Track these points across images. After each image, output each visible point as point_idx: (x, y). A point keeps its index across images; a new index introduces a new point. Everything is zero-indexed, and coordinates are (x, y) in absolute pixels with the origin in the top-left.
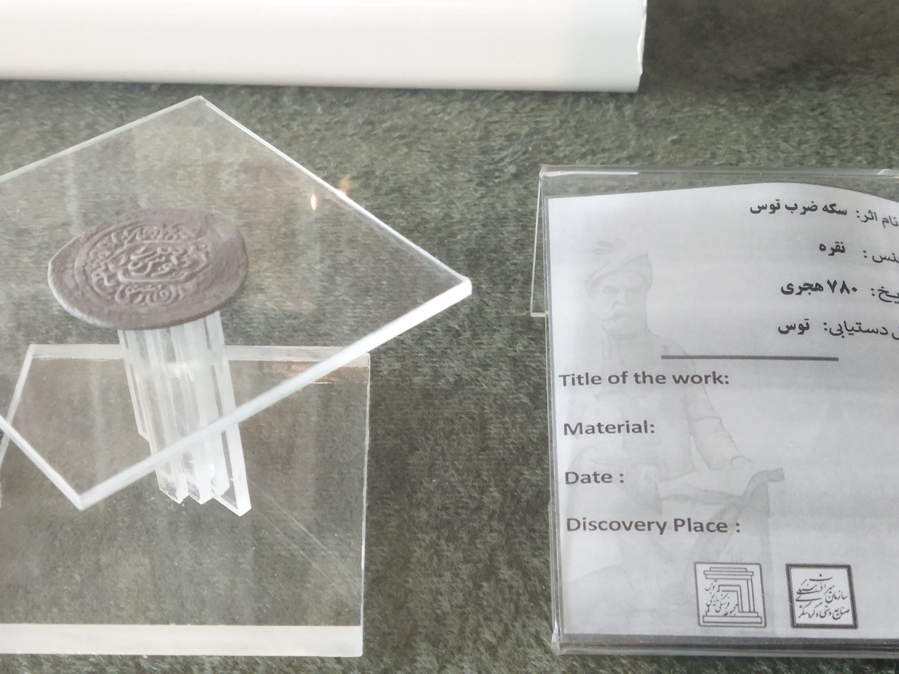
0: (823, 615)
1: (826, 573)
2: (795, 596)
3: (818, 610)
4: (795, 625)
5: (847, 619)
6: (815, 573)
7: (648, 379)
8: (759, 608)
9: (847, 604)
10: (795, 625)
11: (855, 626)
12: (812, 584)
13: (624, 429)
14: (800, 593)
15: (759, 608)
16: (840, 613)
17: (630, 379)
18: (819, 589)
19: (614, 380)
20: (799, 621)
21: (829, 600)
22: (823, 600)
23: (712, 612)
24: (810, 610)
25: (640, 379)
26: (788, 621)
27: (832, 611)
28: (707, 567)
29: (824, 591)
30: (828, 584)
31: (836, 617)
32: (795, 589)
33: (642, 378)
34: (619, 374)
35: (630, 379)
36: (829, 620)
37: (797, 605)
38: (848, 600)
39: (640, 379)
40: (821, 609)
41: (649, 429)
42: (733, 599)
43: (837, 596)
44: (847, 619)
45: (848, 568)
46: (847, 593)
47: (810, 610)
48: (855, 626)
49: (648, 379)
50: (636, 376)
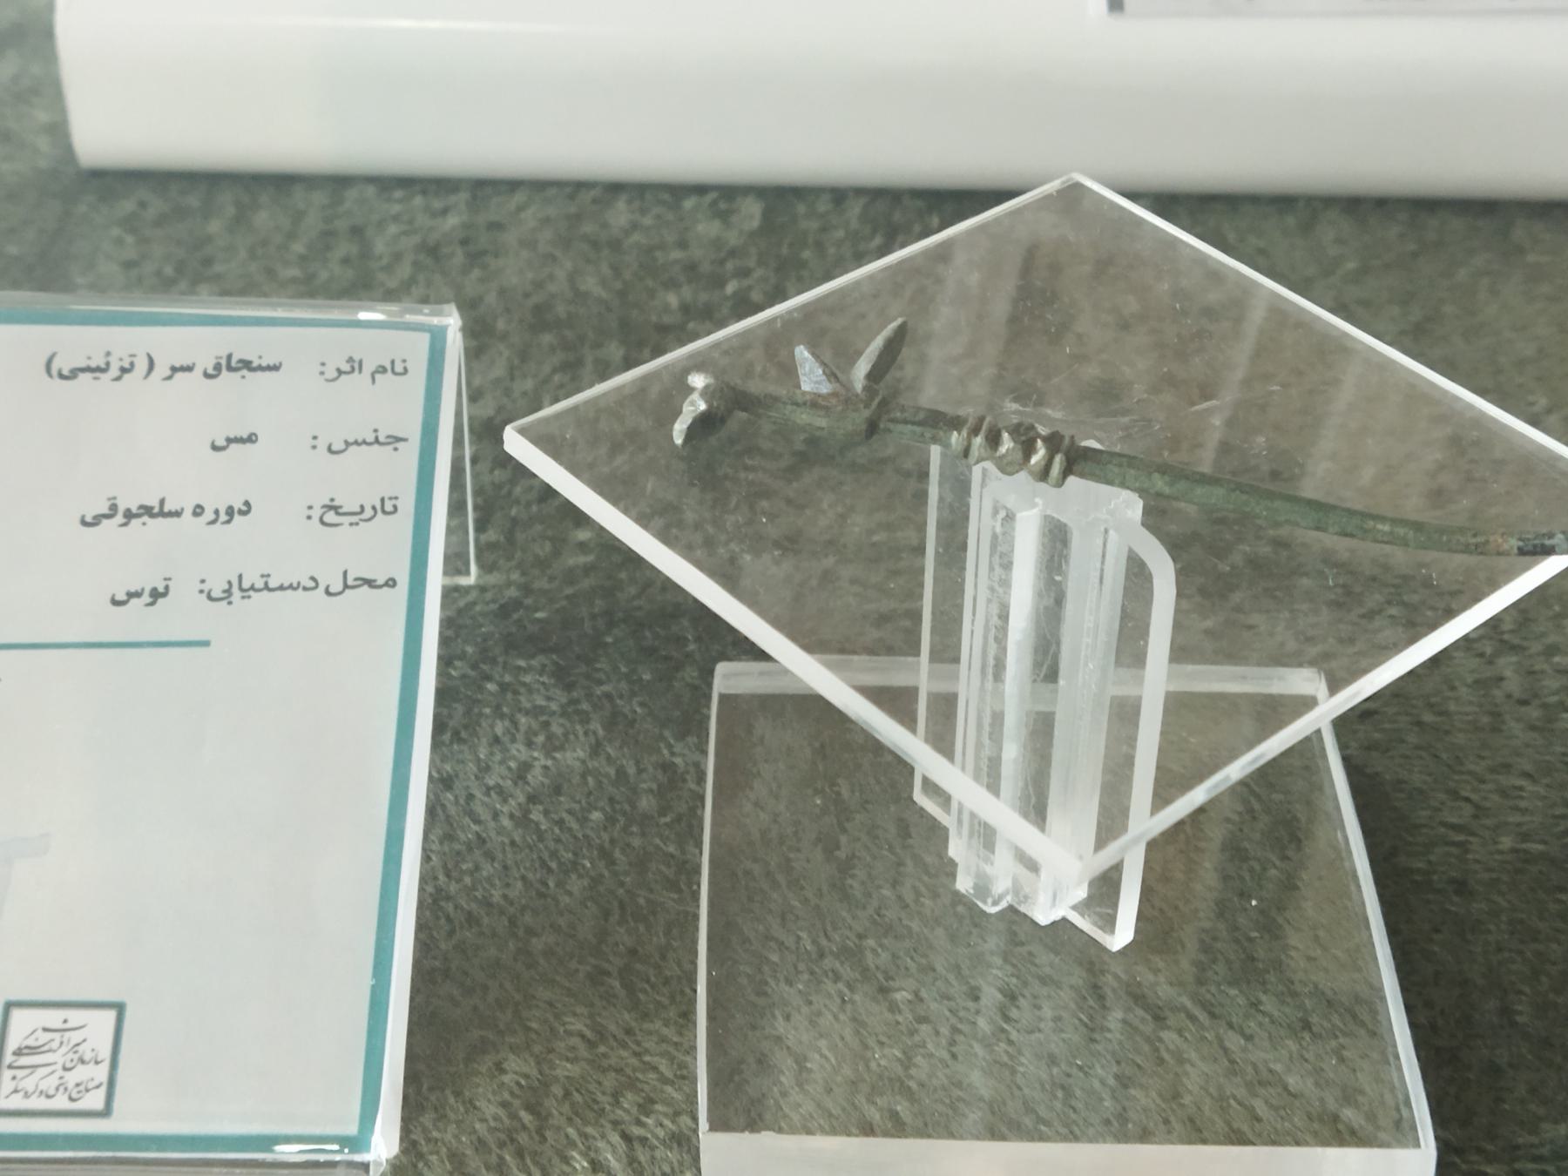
0: (51, 1092)
1: (76, 1017)
3: (43, 1086)
5: (95, 1101)
9: (101, 1073)
11: (106, 1112)
16: (84, 1088)
18: (55, 1045)
21: (69, 1065)
22: (59, 1066)
24: (29, 1084)
27: (71, 1085)
29: (64, 1049)
30: (75, 1037)
31: (74, 1095)
36: (60, 1102)
40: (50, 1084)
43: (87, 1058)
44: (95, 1101)
45: (120, 1008)
46: (105, 1052)
47: (29, 1084)
48: (106, 1112)
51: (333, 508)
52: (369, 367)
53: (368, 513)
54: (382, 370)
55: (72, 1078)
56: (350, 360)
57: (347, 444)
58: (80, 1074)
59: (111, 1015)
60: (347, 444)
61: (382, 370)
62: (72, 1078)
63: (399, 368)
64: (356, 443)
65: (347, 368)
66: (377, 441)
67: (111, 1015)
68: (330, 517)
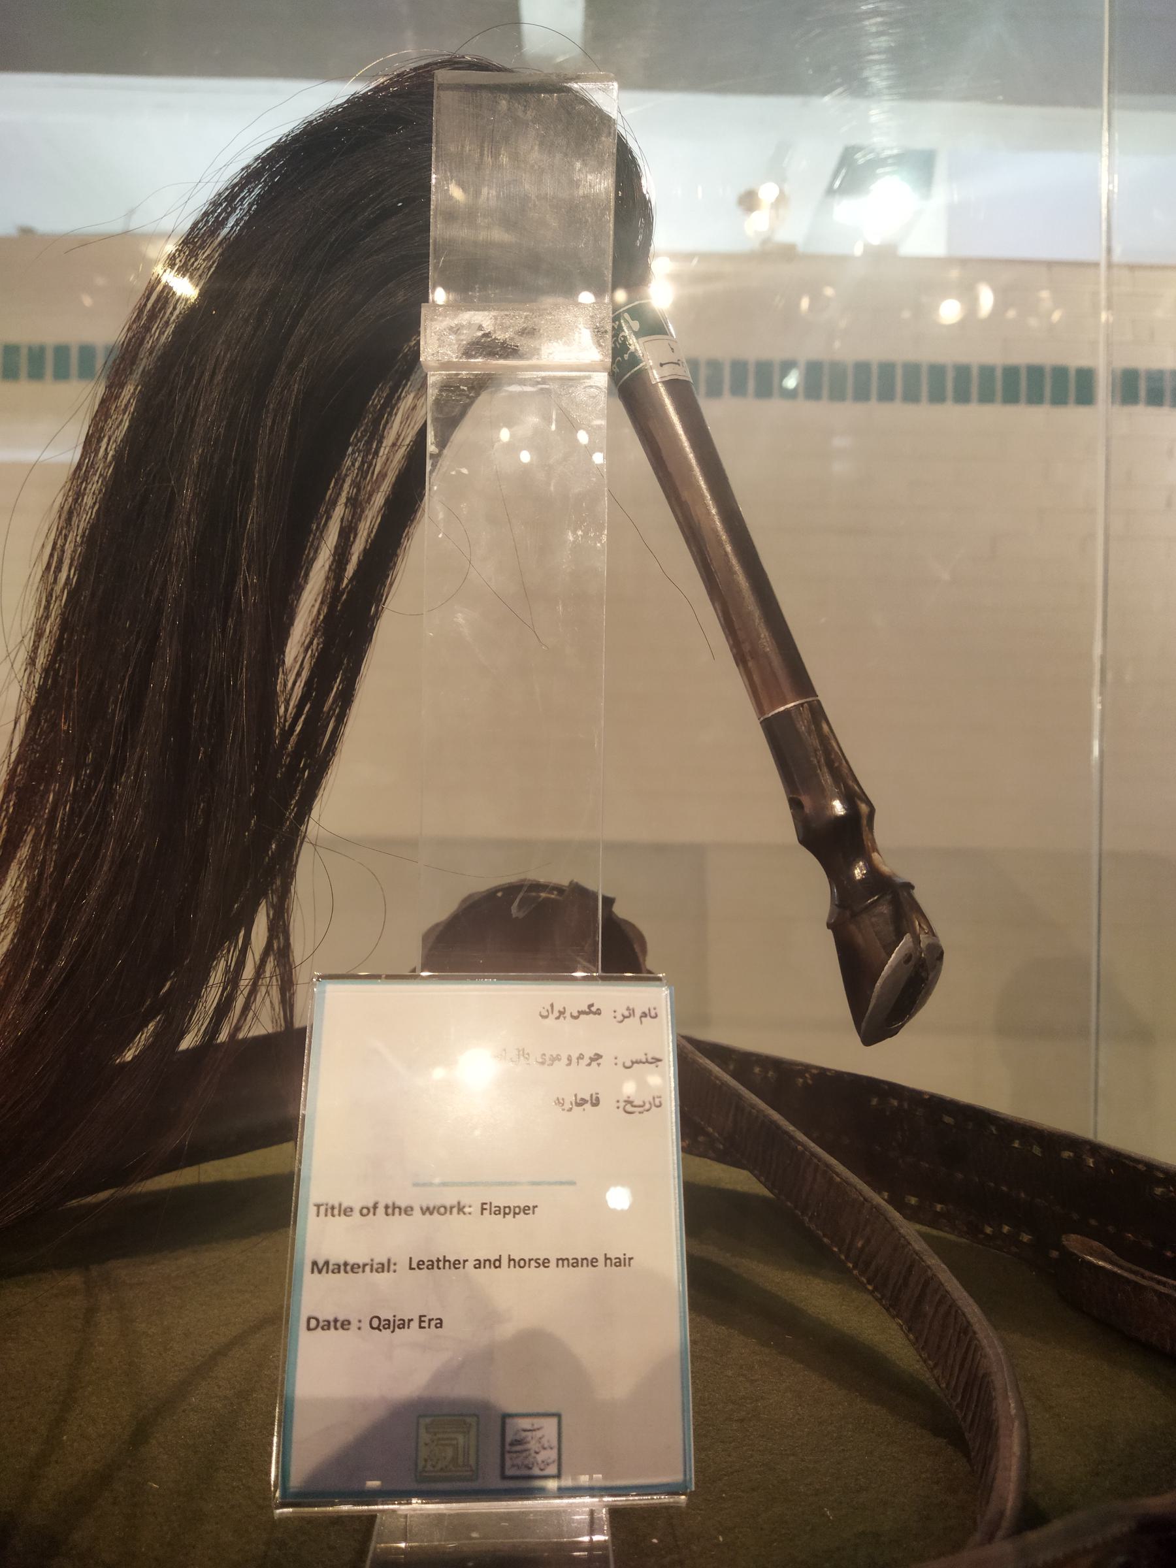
1: (538, 1422)
2: (508, 1448)
4: (504, 1477)
7: (397, 1210)
8: (472, 1462)
9: (553, 1454)
13: (368, 1268)
14: (512, 1444)
15: (472, 1462)
17: (381, 1210)
19: (365, 1211)
23: (429, 1467)
25: (390, 1211)
26: (497, 1472)
28: (428, 1420)
30: (538, 1434)
33: (392, 1209)
34: (371, 1205)
35: (381, 1210)
37: (507, 1456)
38: (555, 1451)
39: (390, 1211)
41: (392, 1267)
42: (450, 1453)
45: (558, 1416)
46: (555, 1443)
49: (397, 1210)
50: (387, 1207)
52: (638, 1013)
53: (647, 1106)
54: (644, 1015)
56: (628, 1009)
57: (633, 1063)
59: (554, 1421)
60: (633, 1063)
61: (644, 1015)
63: (653, 1014)
64: (637, 1062)
65: (626, 1013)
66: (647, 1062)
67: (554, 1421)
68: (629, 1108)
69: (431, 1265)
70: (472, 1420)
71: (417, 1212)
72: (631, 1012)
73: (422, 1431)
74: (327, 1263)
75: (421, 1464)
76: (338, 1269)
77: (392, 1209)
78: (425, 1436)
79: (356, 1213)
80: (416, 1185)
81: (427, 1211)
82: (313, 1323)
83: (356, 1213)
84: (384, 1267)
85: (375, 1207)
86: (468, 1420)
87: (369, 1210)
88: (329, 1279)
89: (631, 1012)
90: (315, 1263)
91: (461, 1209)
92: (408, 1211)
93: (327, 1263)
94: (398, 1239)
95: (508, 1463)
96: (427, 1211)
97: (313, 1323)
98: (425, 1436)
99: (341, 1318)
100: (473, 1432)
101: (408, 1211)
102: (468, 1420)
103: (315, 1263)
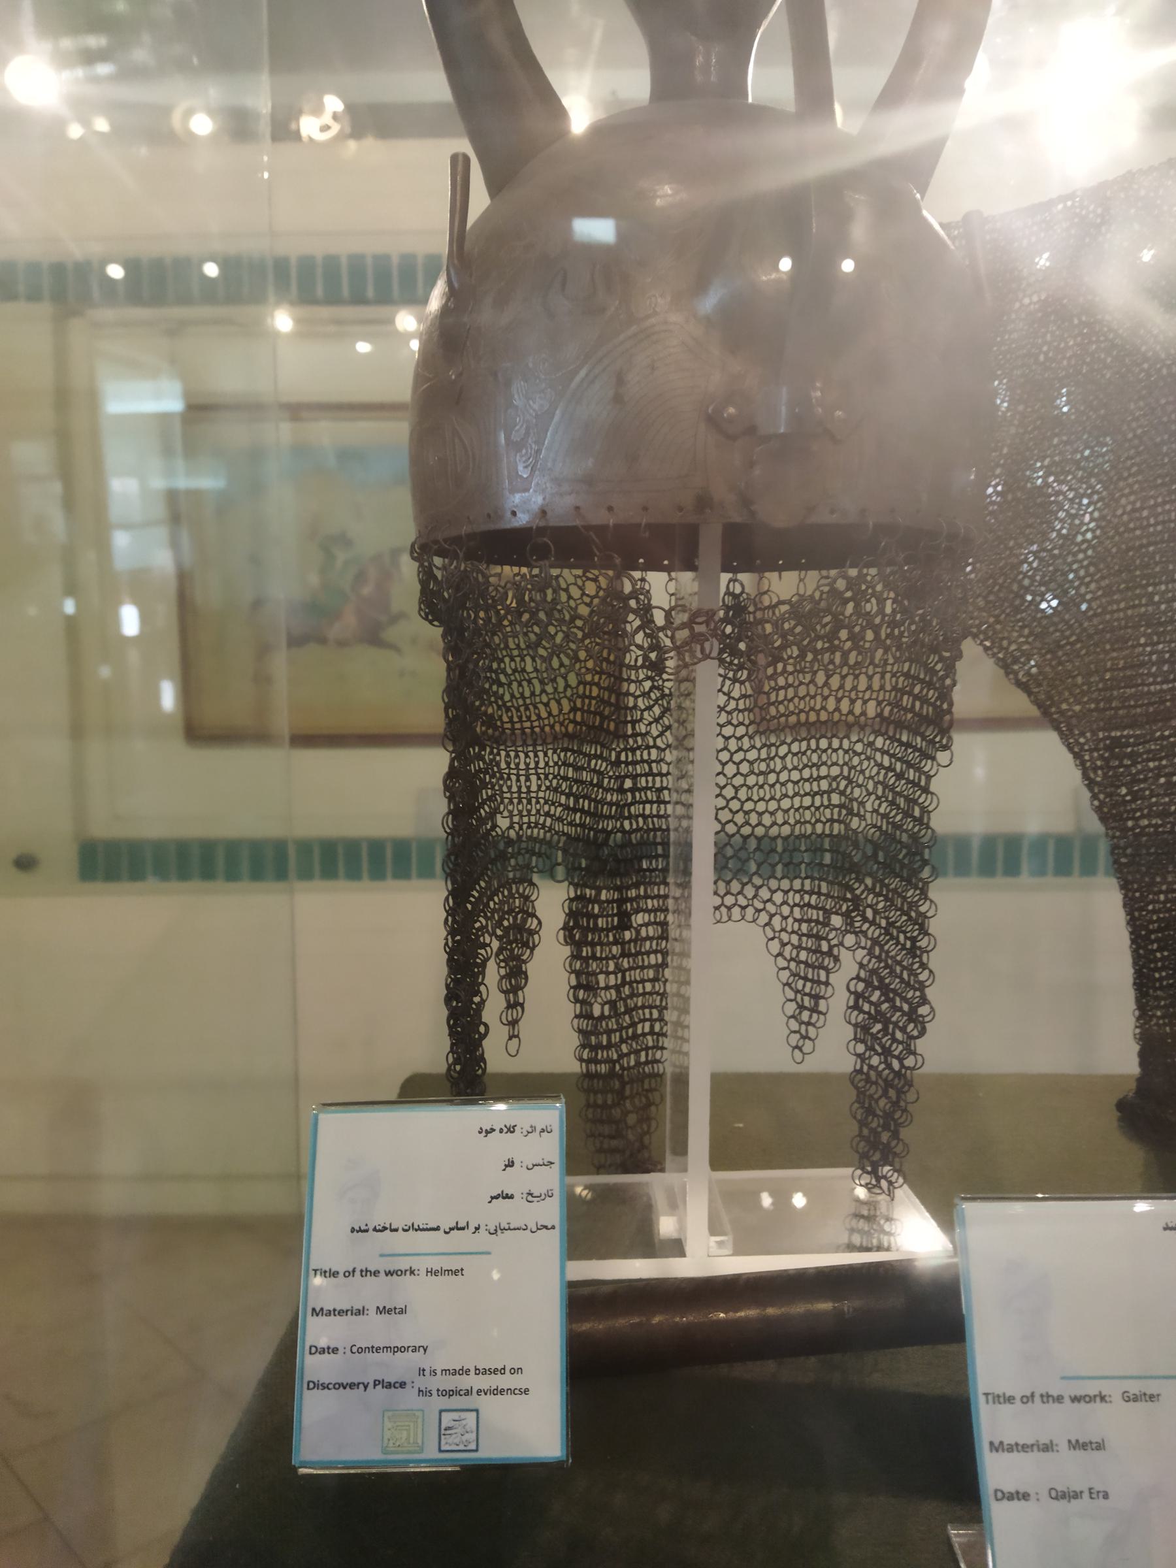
1: (463, 1415)
4: (440, 1451)
6: (455, 1415)
8: (420, 1441)
9: (474, 1435)
10: (440, 1451)
11: (476, 1450)
12: (452, 1424)
15: (420, 1441)
17: (358, 1273)
20: (443, 1448)
28: (390, 1414)
32: (443, 1426)
33: (365, 1272)
35: (358, 1273)
36: (461, 1447)
40: (457, 1441)
42: (405, 1434)
45: (477, 1411)
47: (450, 1441)
51: (530, 1194)
52: (538, 1130)
54: (543, 1131)
55: (464, 1438)
58: (467, 1436)
59: (474, 1414)
61: (543, 1131)
62: (464, 1438)
67: (474, 1414)
68: (530, 1198)
69: (389, 1311)
70: (419, 1414)
71: (382, 1274)
72: (533, 1129)
73: (386, 1419)
74: (322, 1309)
75: (386, 1441)
76: (329, 1313)
77: (365, 1272)
78: (388, 1424)
79: (341, 1274)
80: (382, 1255)
81: (389, 1273)
82: (313, 1350)
83: (341, 1274)
84: (360, 1312)
85: (354, 1271)
86: (417, 1413)
87: (350, 1273)
88: (323, 1320)
89: (533, 1129)
90: (314, 1310)
91: (412, 1272)
92: (376, 1273)
93: (322, 1309)
94: (370, 1292)
95: (443, 1442)
96: (389, 1273)
97: (313, 1350)
98: (388, 1424)
99: (332, 1346)
100: (420, 1420)
101: (376, 1273)
102: (417, 1413)
103: (314, 1310)
